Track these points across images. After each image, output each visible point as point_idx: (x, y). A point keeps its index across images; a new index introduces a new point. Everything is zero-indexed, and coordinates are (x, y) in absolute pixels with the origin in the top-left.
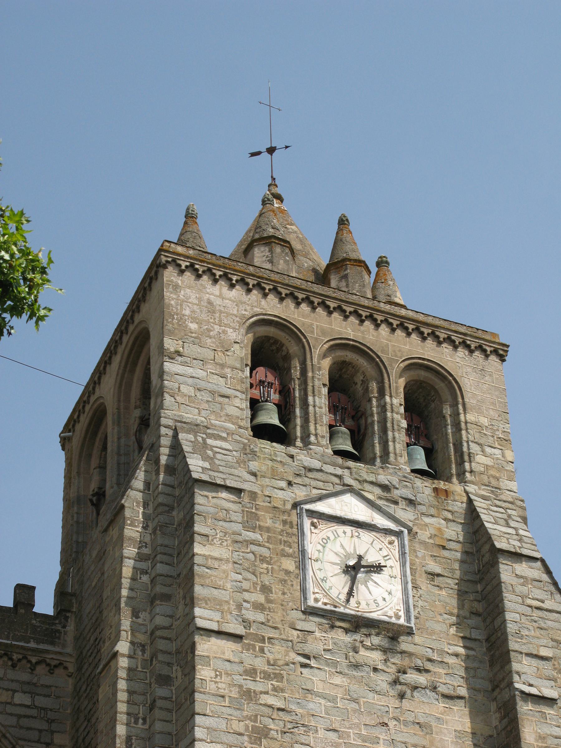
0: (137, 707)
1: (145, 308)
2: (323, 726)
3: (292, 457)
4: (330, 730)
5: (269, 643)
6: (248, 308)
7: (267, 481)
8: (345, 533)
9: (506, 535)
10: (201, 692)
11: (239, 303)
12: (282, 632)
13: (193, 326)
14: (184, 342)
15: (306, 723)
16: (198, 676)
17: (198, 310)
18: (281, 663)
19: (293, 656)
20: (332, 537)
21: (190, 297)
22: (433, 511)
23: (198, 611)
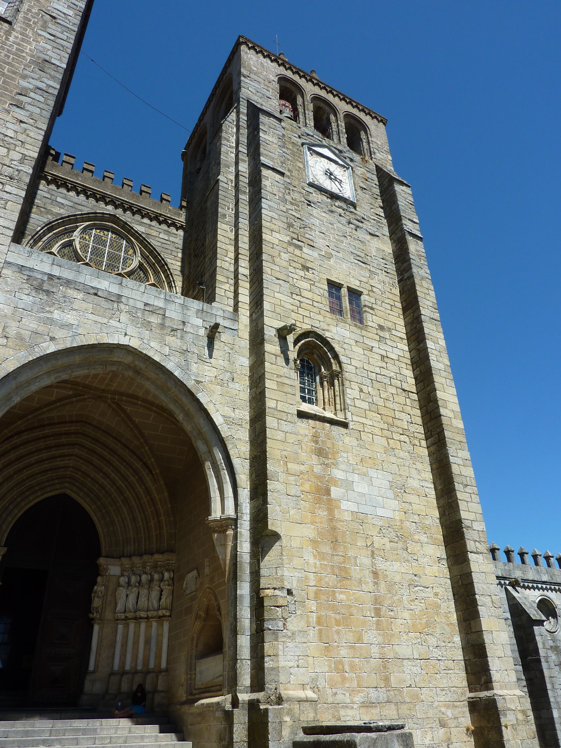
1: (229, 71)
7: (289, 132)
13: (255, 69)
16: (263, 183)
18: (298, 200)
19: (303, 199)
22: (361, 166)
23: (262, 158)
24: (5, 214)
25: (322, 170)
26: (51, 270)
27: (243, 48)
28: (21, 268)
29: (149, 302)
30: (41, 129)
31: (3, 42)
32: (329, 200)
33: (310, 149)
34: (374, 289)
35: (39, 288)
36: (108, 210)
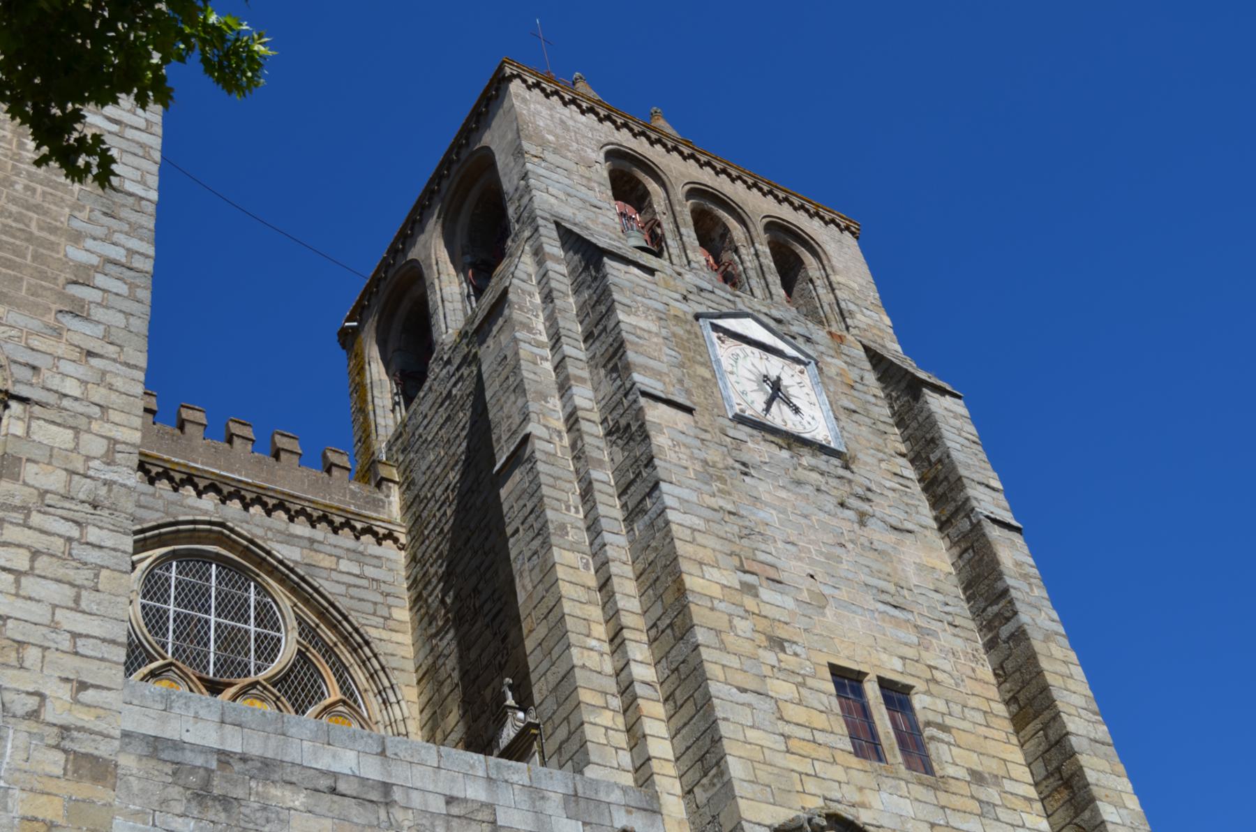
10: (660, 459)
13: (551, 138)
19: (730, 461)
20: (742, 355)
24: (99, 604)
25: (753, 378)
26: (222, 739)
27: (515, 87)
28: (155, 746)
29: (455, 793)
30: (135, 367)
31: (14, 154)
32: (785, 454)
33: (716, 328)
34: (938, 675)
35: (202, 796)
36: (206, 513)
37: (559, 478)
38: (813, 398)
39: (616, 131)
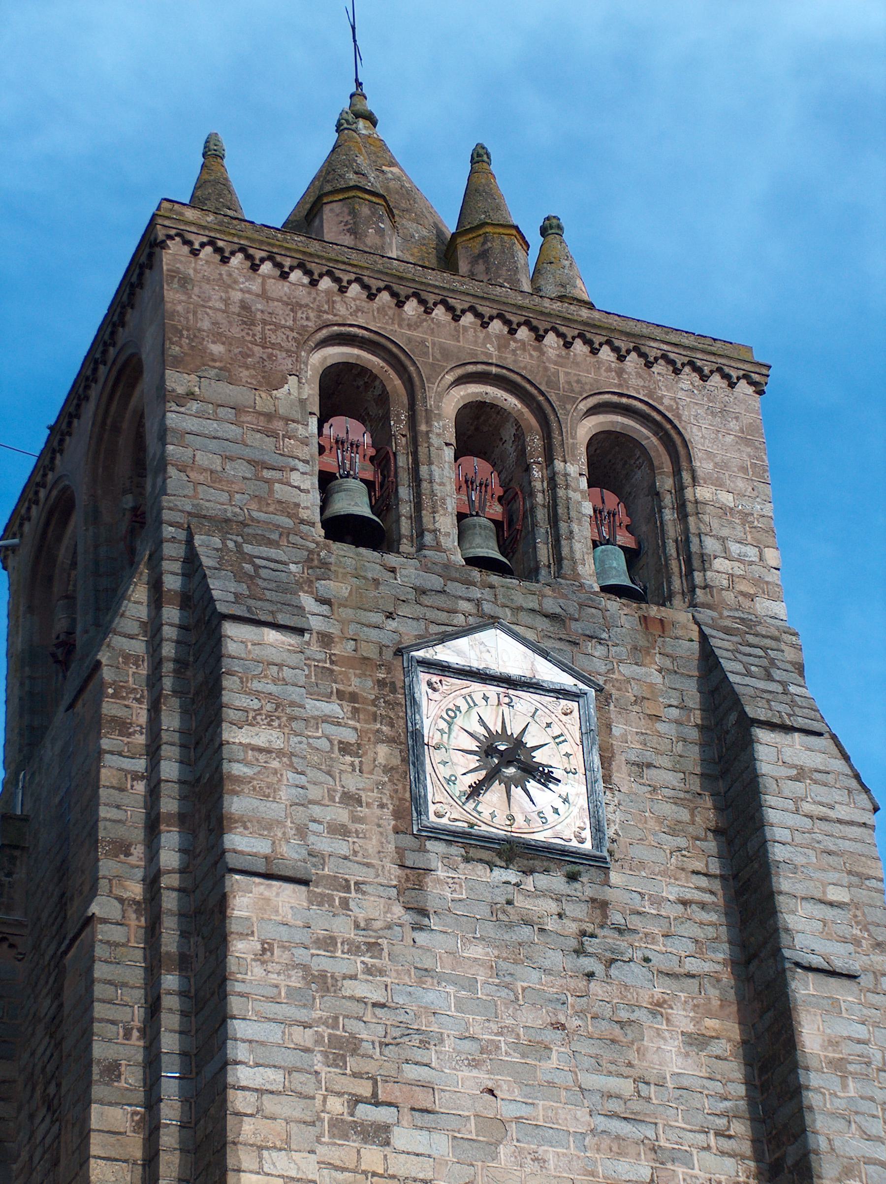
0: (128, 1009)
2: (452, 1032)
3: (393, 570)
4: (466, 1038)
5: (357, 891)
6: (312, 315)
7: (347, 613)
8: (486, 698)
9: (765, 695)
11: (295, 306)
12: (380, 872)
13: (217, 349)
14: (200, 377)
15: (424, 1028)
17: (224, 321)
18: (378, 925)
20: (464, 707)
21: (210, 299)
25: (473, 745)
32: (500, 875)
37: (124, 985)
38: (577, 762)
39: (337, 298)
